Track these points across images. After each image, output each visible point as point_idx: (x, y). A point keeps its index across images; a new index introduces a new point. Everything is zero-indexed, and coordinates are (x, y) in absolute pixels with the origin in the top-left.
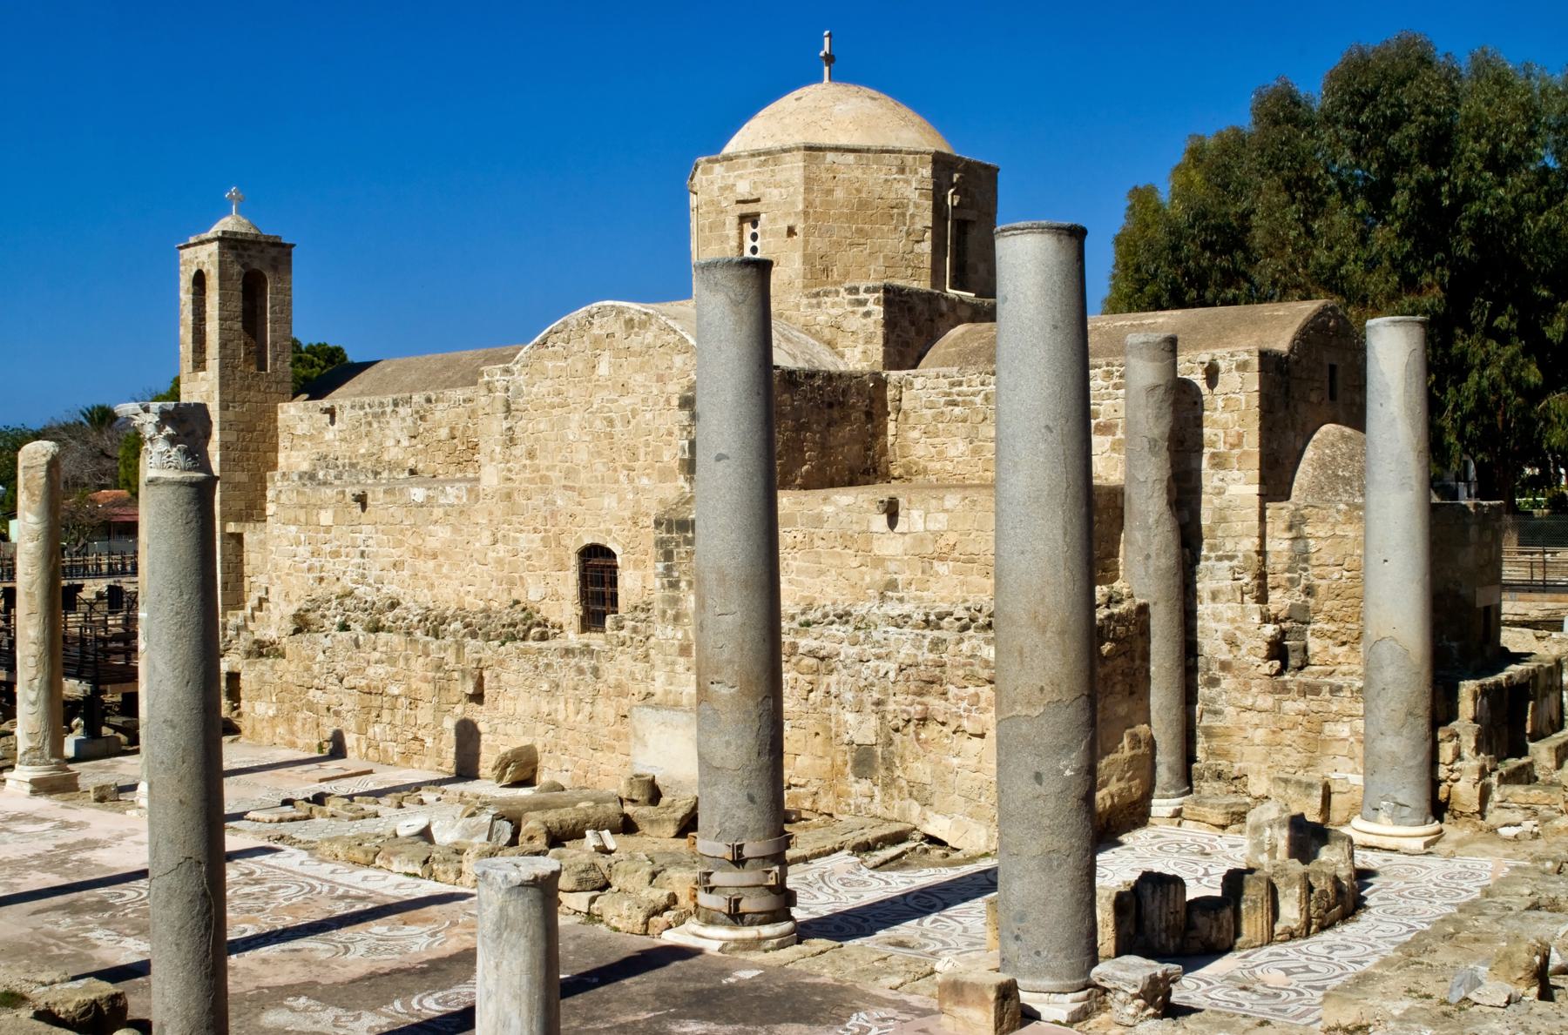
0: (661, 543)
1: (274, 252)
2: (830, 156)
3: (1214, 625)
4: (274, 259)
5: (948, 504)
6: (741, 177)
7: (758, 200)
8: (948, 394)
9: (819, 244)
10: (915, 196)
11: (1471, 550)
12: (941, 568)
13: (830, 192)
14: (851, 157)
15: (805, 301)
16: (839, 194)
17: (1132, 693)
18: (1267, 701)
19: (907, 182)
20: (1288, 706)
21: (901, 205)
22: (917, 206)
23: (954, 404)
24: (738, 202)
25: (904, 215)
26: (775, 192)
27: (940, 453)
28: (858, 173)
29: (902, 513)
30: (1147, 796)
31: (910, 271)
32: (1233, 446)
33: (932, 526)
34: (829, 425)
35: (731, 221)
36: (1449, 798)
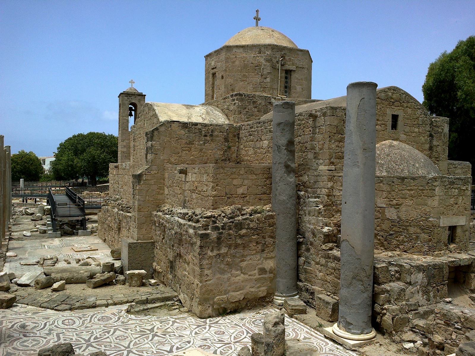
0: (133, 182)
1: (139, 97)
2: (235, 50)
3: (308, 225)
4: (139, 100)
5: (196, 171)
6: (213, 60)
7: (216, 68)
8: (249, 132)
9: (230, 81)
10: (262, 60)
11: (437, 198)
12: (194, 196)
13: (234, 62)
14: (241, 50)
15: (222, 101)
16: (237, 63)
17: (263, 251)
18: (323, 261)
19: (261, 57)
20: (329, 264)
21: (258, 66)
22: (265, 65)
23: (250, 135)
24: (213, 69)
25: (260, 69)
26: (219, 64)
27: (247, 153)
28: (244, 55)
29: (188, 174)
30: (273, 294)
31: (262, 89)
32: (321, 149)
33: (193, 179)
34: (204, 143)
35: (211, 76)
36: (381, 321)
